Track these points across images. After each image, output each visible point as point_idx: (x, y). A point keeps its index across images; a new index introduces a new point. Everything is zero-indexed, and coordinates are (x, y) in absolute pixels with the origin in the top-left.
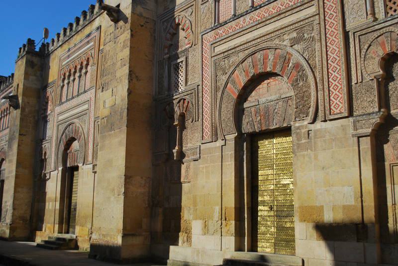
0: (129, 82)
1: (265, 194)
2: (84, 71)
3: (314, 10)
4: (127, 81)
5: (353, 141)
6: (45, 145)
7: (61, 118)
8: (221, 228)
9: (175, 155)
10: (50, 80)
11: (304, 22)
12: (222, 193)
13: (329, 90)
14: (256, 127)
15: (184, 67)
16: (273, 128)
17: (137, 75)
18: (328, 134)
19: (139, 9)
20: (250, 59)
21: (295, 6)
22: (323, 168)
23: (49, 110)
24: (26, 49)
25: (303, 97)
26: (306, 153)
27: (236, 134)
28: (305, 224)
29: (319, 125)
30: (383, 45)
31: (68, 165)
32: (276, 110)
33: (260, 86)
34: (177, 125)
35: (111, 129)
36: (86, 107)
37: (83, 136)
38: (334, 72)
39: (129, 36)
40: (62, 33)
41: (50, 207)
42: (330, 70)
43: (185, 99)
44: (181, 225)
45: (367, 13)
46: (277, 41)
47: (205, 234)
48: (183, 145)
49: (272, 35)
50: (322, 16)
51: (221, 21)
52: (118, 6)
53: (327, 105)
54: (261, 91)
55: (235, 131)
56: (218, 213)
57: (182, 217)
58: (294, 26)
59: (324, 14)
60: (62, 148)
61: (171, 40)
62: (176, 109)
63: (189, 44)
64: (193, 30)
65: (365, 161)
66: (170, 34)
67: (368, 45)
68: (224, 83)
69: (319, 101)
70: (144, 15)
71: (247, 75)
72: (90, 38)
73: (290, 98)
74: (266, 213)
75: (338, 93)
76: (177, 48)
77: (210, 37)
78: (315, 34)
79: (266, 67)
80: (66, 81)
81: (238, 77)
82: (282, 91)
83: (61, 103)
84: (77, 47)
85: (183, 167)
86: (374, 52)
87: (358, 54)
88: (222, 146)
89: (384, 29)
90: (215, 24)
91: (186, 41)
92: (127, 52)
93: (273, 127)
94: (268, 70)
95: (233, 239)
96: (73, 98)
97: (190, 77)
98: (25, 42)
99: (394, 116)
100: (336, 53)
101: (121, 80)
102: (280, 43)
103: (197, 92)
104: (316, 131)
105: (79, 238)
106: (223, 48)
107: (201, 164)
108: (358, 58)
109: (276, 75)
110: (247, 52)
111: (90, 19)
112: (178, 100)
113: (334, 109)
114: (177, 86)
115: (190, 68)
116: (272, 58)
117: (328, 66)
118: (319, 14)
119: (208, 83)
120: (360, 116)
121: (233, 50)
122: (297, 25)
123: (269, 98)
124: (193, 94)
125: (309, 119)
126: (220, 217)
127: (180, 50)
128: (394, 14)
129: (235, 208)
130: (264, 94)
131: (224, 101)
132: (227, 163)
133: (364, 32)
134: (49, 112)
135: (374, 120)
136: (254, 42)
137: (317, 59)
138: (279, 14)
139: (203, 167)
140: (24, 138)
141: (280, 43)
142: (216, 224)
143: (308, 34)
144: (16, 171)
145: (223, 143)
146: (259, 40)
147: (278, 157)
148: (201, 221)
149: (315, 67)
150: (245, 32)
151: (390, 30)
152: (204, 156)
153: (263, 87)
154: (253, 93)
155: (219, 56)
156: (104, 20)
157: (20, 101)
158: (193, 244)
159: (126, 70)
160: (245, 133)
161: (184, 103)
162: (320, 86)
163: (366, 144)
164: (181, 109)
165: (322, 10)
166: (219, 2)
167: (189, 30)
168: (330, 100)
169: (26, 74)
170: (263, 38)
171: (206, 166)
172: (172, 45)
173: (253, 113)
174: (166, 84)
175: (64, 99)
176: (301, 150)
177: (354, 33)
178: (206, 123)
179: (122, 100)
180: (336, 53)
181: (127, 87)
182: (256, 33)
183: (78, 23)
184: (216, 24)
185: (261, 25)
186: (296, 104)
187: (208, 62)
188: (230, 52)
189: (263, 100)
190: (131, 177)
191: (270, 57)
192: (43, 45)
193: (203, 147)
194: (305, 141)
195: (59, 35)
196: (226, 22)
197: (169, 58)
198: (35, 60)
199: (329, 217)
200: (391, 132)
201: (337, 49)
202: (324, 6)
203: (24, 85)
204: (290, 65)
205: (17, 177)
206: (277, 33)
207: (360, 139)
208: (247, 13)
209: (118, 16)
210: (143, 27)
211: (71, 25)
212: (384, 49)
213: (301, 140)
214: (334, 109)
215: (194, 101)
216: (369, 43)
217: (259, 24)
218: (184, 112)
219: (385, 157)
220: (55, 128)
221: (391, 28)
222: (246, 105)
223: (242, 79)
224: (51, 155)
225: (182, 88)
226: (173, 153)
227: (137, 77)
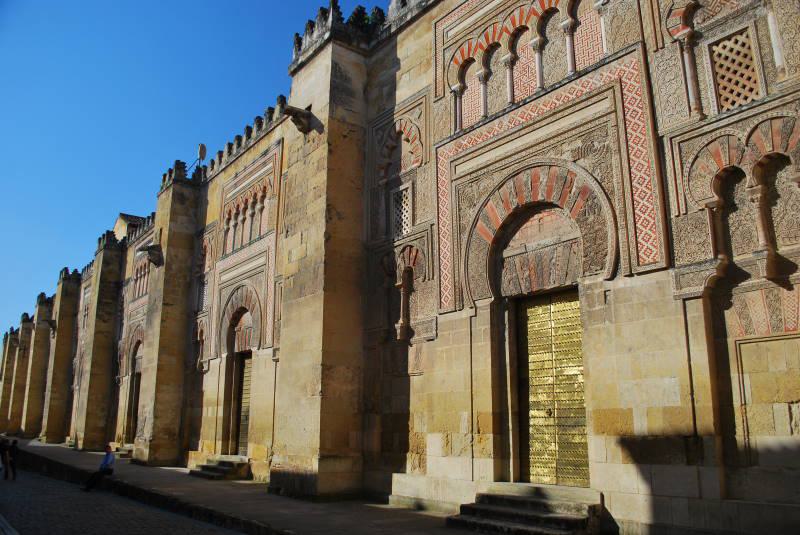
0: (327, 221)
1: (540, 391)
2: (258, 206)
4: (324, 221)
5: (676, 305)
6: (202, 319)
7: (225, 278)
9: (398, 331)
10: (209, 221)
11: (593, 124)
13: (635, 228)
14: (523, 288)
15: (409, 201)
17: (339, 210)
19: (340, 112)
20: (510, 183)
21: (577, 100)
22: (630, 350)
23: (207, 266)
24: (173, 175)
25: (595, 240)
26: (601, 326)
28: (603, 438)
29: (621, 282)
30: (716, 155)
31: (236, 350)
32: (554, 261)
33: (528, 224)
34: (400, 286)
35: (301, 294)
36: (262, 260)
37: (257, 304)
38: (642, 199)
39: (326, 153)
40: (226, 150)
41: (210, 415)
42: (636, 197)
43: (411, 247)
45: (690, 108)
46: (552, 155)
49: (545, 145)
50: (620, 114)
51: (465, 126)
52: (309, 108)
53: (633, 251)
54: (529, 232)
55: (490, 294)
58: (578, 130)
59: (624, 111)
60: (227, 323)
61: (390, 156)
62: (399, 261)
63: (417, 161)
64: (423, 140)
65: (695, 337)
66: (387, 147)
67: (693, 157)
68: (472, 220)
69: (621, 245)
70: (348, 120)
71: (506, 203)
72: (268, 156)
73: (574, 241)
74: (541, 422)
75: (649, 232)
76: (399, 168)
77: (448, 151)
78: (610, 142)
79: (535, 194)
80: (232, 223)
81: (493, 210)
82: (561, 231)
83: (225, 256)
84: (248, 171)
85: (412, 351)
86: (703, 168)
87: (678, 171)
89: (718, 131)
90: (455, 130)
91: (413, 158)
92: (323, 176)
96: (242, 247)
97: (419, 212)
98: (171, 165)
99: (739, 266)
100: (643, 170)
101: (314, 220)
103: (430, 234)
104: (617, 292)
105: (252, 462)
106: (470, 166)
107: (439, 346)
108: (679, 177)
109: (551, 205)
110: (506, 172)
111: (266, 129)
112: (402, 247)
113: (645, 257)
114: (399, 226)
115: (419, 197)
117: (632, 191)
118: (615, 111)
119: (447, 221)
120: (686, 266)
122: (582, 129)
123: (543, 242)
124: (425, 238)
125: (606, 273)
127: (403, 171)
128: (731, 107)
129: (493, 413)
130: (534, 236)
133: (686, 136)
134: (207, 269)
136: (516, 157)
137: (614, 180)
138: (555, 113)
140: (169, 308)
144: (159, 360)
145: (473, 311)
146: (524, 153)
147: (560, 333)
149: (613, 192)
150: (502, 142)
151: (727, 133)
154: (517, 235)
155: (463, 180)
156: (288, 130)
157: (165, 254)
158: (428, 470)
159: (321, 205)
161: (410, 251)
162: (621, 222)
163: (697, 310)
164: (407, 262)
165: (619, 105)
166: (461, 98)
167: (417, 142)
168: (637, 243)
169: (174, 213)
170: (531, 151)
172: (390, 164)
175: (229, 250)
177: (671, 139)
178: (445, 283)
179: (317, 249)
180: (643, 170)
181: (324, 230)
182: (519, 144)
183: (249, 136)
184: (458, 131)
185: (527, 130)
186: (584, 250)
187: (447, 189)
189: (532, 245)
192: (198, 169)
193: (441, 319)
194: (600, 307)
195: (221, 154)
196: (472, 127)
197: (387, 184)
198: (187, 192)
199: (641, 426)
200: (735, 291)
201: (646, 164)
202: (622, 98)
203: (170, 230)
204: (574, 189)
205: (160, 369)
206: (552, 141)
207: (687, 302)
208: (504, 112)
209: (309, 124)
210: (347, 139)
211: (239, 138)
212: (719, 162)
214: (645, 257)
215: (426, 249)
216: (695, 153)
217: (524, 128)
218: (411, 265)
219: (728, 330)
220: (217, 294)
221: (728, 129)
222: (506, 253)
223: (499, 214)
224: (210, 333)
225: (407, 229)
226: (395, 330)
227: (338, 214)
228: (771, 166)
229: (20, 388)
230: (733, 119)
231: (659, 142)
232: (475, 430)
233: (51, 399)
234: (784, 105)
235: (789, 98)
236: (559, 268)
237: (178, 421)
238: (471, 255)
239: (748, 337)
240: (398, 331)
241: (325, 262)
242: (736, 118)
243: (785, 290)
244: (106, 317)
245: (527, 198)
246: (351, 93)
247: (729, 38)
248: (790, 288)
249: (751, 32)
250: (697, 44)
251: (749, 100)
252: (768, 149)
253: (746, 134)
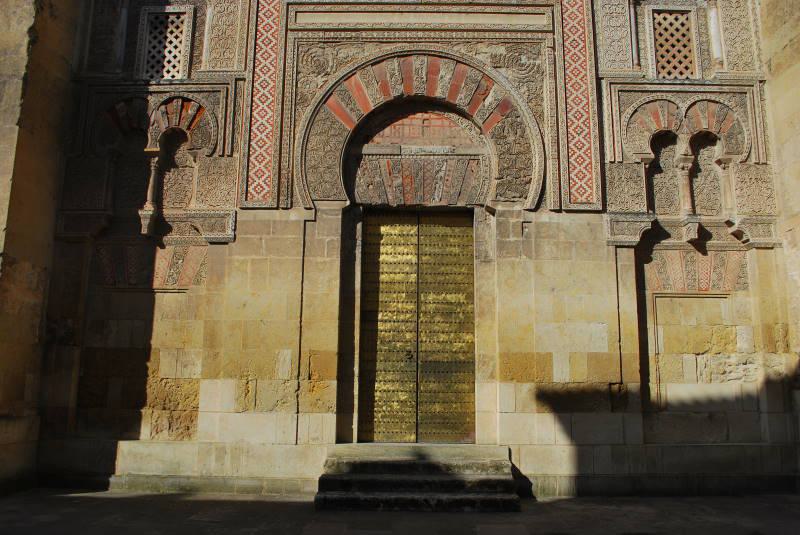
3: (545, 22)
5: (608, 250)
8: (297, 396)
9: (145, 223)
11: (524, 36)
12: (301, 321)
15: (186, 28)
16: (433, 204)
18: (563, 233)
26: (518, 260)
27: (348, 203)
29: (545, 216)
30: (656, 115)
32: (441, 174)
34: (153, 154)
43: (186, 100)
44: (148, 391)
47: (245, 410)
48: (165, 203)
49: (454, 34)
55: (344, 195)
56: (288, 359)
57: (150, 372)
58: (503, 35)
65: (624, 284)
68: (319, 94)
71: (384, 88)
81: (359, 89)
82: (456, 141)
85: (162, 259)
86: (641, 122)
88: (305, 221)
93: (435, 202)
94: (438, 94)
102: (470, 54)
103: (229, 89)
104: (539, 226)
106: (322, 21)
110: (388, 48)
112: (165, 97)
113: (577, 195)
114: (157, 64)
116: (448, 77)
118: (553, 32)
121: (354, 34)
122: (508, 35)
123: (429, 148)
124: (222, 95)
125: (529, 203)
126: (296, 373)
128: (679, 77)
131: (316, 129)
132: (319, 259)
133: (628, 87)
135: (643, 225)
136: (408, 34)
139: (244, 262)
141: (470, 54)
142: (282, 387)
143: (529, 58)
145: (310, 215)
146: (420, 34)
148: (232, 382)
149: (541, 115)
151: (668, 98)
152: (249, 236)
153: (410, 125)
154: (387, 130)
160: (362, 204)
170: (432, 34)
171: (253, 260)
173: (384, 169)
174: (119, 48)
176: (507, 253)
185: (429, 8)
188: (343, 34)
189: (408, 148)
191: (442, 73)
193: (243, 216)
194: (515, 239)
199: (562, 375)
200: (656, 247)
204: (489, 99)
213: (508, 237)
214: (577, 195)
221: (670, 95)
222: (367, 149)
223: (373, 99)
226: (138, 219)
228: (702, 140)
230: (674, 88)
231: (599, 80)
232: (304, 374)
234: (720, 93)
235: (726, 89)
236: (448, 183)
238: (314, 141)
239: (666, 291)
240: (145, 223)
241: (25, 79)
242: (678, 88)
243: (700, 255)
245: (418, 88)
247: (671, 12)
248: (705, 253)
249: (692, 16)
250: (640, 5)
251: (684, 77)
252: (705, 126)
253: (687, 106)
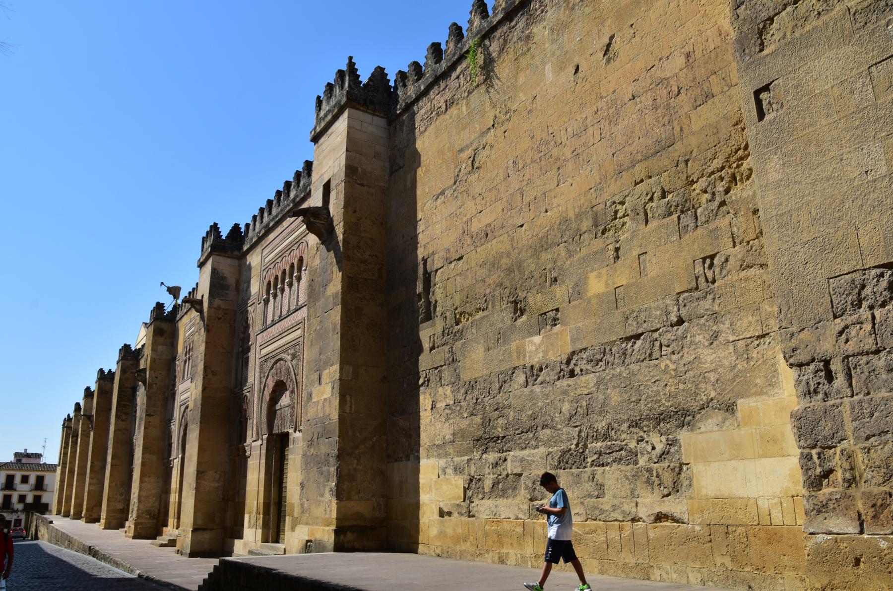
70: (223, 306)
95: (261, 530)
140: (151, 419)
144: (143, 458)
169: (154, 344)
190: (203, 472)
210: (221, 320)
227: (212, 371)
229: (72, 472)
233: (89, 484)
237: (157, 504)
244: (124, 417)
246: (226, 288)
